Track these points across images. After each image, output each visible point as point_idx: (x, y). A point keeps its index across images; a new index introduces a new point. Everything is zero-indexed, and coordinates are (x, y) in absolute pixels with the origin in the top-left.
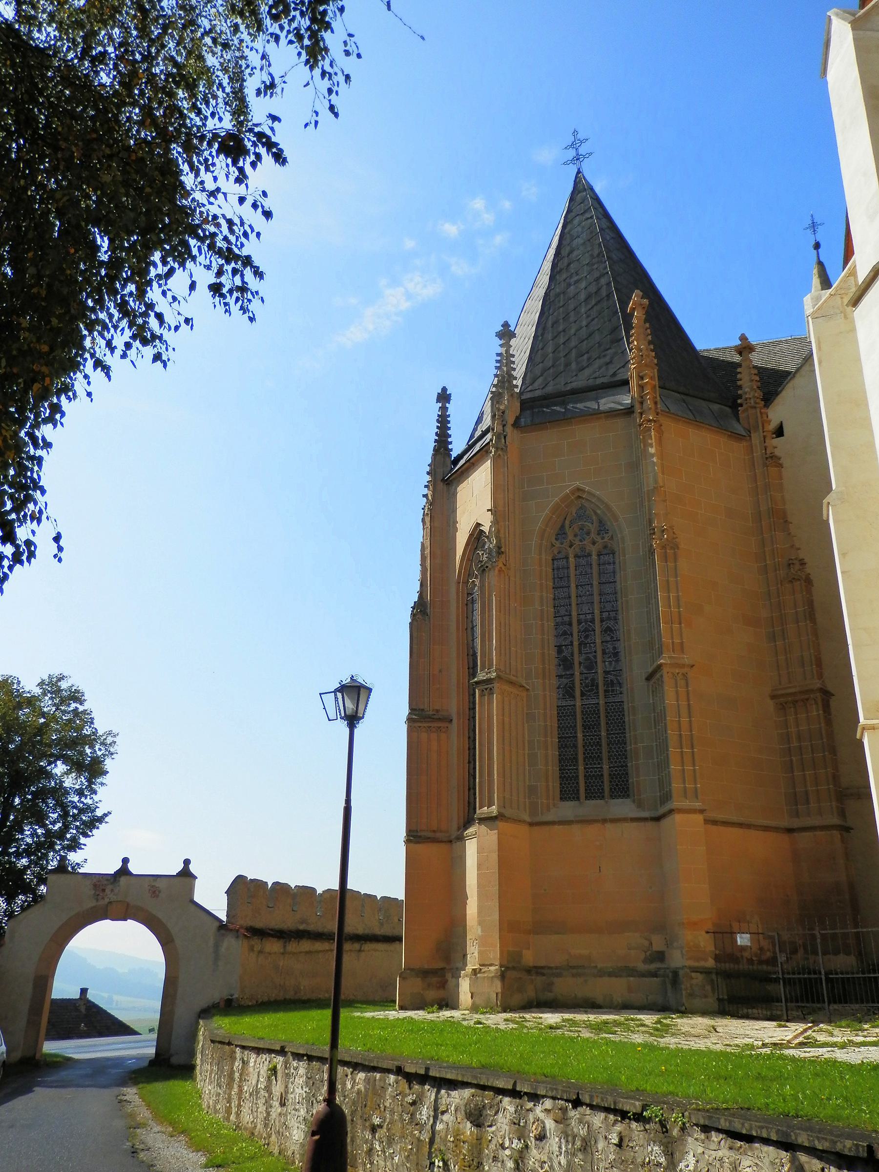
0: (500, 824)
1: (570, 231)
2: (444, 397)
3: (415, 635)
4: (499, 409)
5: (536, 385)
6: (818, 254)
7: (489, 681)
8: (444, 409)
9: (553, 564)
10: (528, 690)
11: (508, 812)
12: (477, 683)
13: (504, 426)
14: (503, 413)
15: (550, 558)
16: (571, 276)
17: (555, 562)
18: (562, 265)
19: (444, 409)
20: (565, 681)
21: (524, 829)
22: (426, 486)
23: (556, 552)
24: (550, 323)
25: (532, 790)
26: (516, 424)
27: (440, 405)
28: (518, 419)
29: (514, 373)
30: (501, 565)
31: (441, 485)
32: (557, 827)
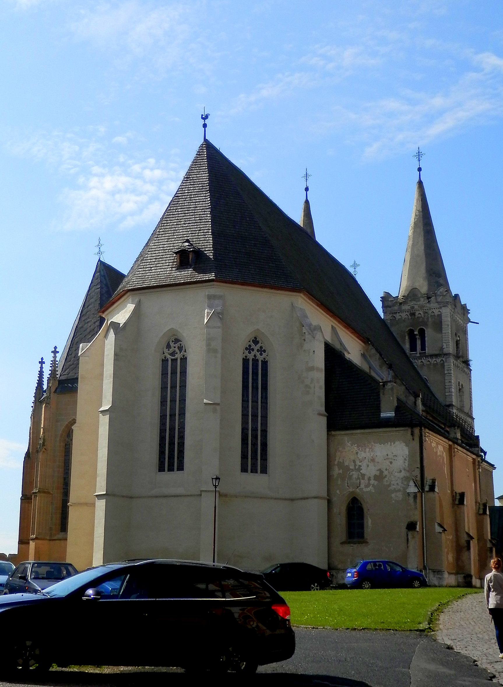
0: (37, 541)
1: (90, 294)
2: (42, 362)
3: (25, 466)
4: (49, 386)
5: (66, 372)
6: (307, 193)
7: (36, 493)
8: (41, 368)
9: (65, 447)
10: (52, 494)
11: (39, 537)
12: (33, 493)
13: (50, 393)
14: (51, 387)
15: (64, 445)
16: (86, 319)
17: (66, 446)
18: (84, 313)
19: (41, 368)
20: (65, 490)
21: (47, 542)
22: (33, 403)
23: (66, 443)
24: (75, 343)
25: (51, 529)
26: (55, 392)
27: (43, 361)
28: (57, 389)
29: (57, 369)
30: (44, 450)
31: (38, 403)
32: (57, 541)
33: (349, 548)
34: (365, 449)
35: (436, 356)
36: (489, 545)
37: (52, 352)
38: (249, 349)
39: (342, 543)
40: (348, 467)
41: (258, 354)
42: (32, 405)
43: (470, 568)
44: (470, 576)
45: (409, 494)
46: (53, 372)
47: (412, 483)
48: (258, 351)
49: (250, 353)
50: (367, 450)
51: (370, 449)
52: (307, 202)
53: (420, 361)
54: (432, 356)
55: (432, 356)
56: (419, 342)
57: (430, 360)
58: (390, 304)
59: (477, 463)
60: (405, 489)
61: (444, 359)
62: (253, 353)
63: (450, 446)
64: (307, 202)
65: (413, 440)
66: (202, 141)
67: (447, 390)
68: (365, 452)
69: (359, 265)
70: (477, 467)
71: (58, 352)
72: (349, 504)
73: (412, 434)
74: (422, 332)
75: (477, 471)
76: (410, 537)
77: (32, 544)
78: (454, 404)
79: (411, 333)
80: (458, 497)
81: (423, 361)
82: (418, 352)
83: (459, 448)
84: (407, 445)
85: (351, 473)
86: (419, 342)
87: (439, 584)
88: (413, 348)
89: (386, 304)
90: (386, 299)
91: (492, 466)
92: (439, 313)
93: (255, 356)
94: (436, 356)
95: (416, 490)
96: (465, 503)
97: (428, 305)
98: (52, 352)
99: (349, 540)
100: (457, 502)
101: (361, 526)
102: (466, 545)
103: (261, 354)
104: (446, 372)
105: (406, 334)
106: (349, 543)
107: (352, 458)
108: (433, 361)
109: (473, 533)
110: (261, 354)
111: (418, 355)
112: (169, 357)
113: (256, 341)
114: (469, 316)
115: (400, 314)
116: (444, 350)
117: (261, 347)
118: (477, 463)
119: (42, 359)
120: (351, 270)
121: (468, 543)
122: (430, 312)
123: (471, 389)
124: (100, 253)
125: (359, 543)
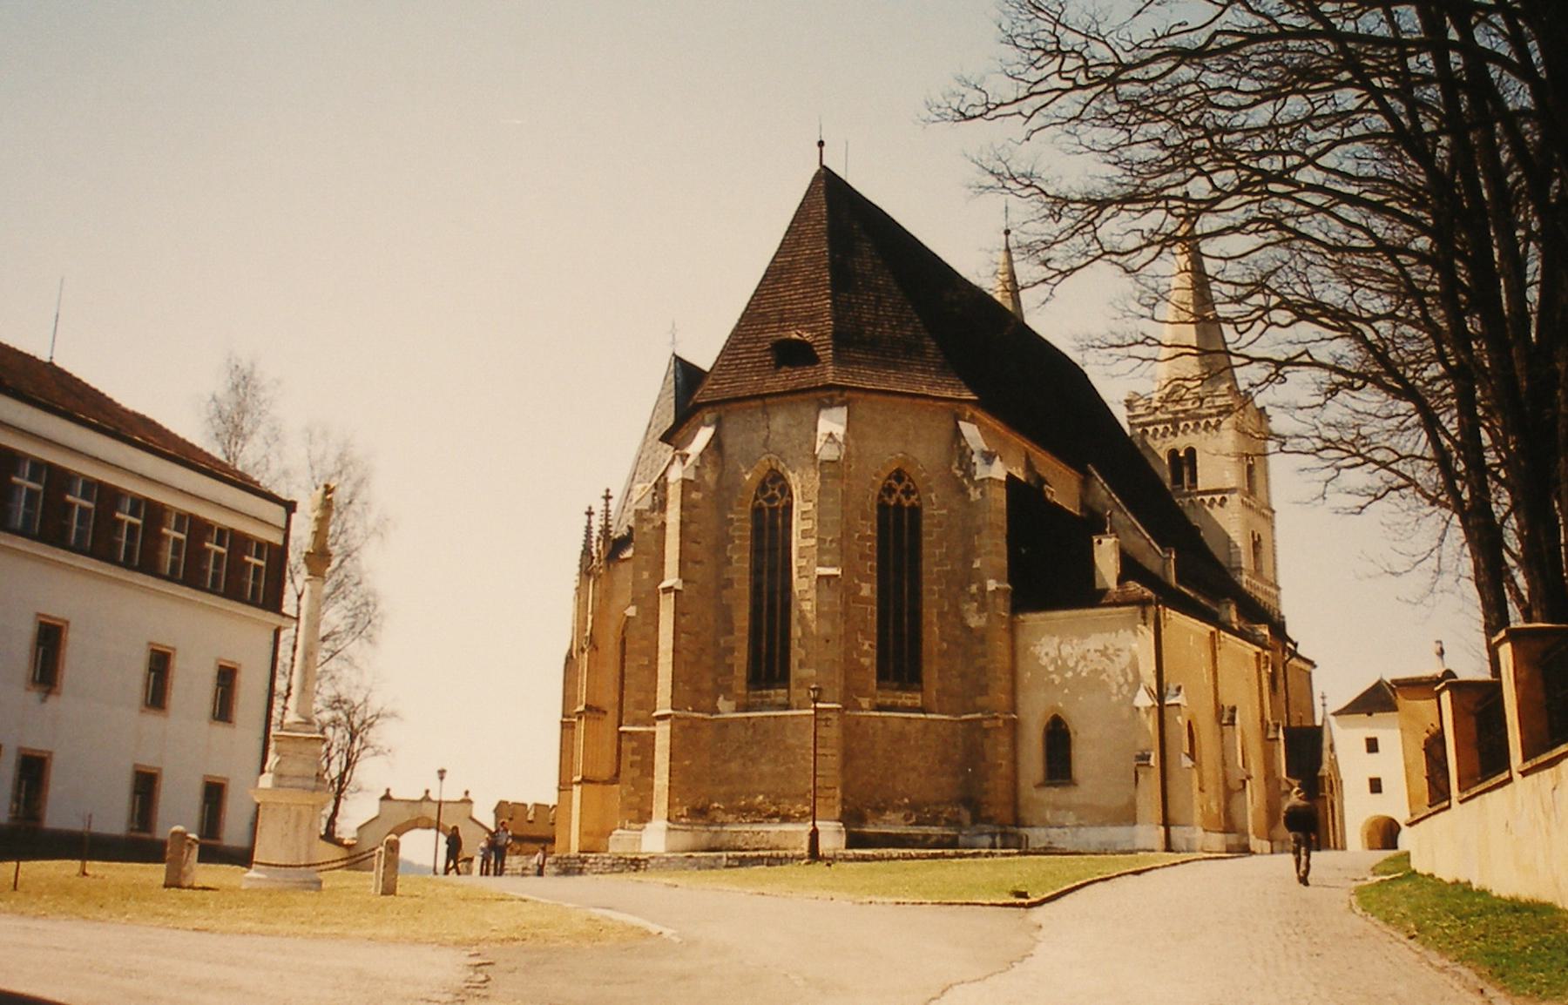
2: (590, 513)
8: (589, 522)
19: (589, 522)
38: (889, 490)
41: (903, 497)
43: (1246, 822)
44: (1246, 834)
46: (606, 530)
48: (902, 492)
49: (890, 496)
53: (1188, 499)
55: (1206, 492)
56: (1186, 470)
59: (1262, 660)
62: (894, 497)
63: (1212, 633)
66: (817, 167)
71: (611, 497)
73: (1144, 617)
74: (1191, 452)
75: (1263, 672)
76: (1141, 777)
77: (577, 790)
80: (1227, 714)
82: (1186, 485)
83: (1228, 636)
86: (1186, 470)
91: (1311, 663)
93: (899, 500)
95: (1150, 703)
96: (1237, 721)
98: (603, 497)
103: (908, 498)
106: (1048, 785)
107: (1053, 653)
109: (1256, 768)
110: (908, 498)
111: (1186, 490)
112: (765, 504)
113: (899, 475)
114: (1270, 425)
117: (908, 486)
118: (1262, 660)
119: (590, 508)
121: (1244, 782)
124: (673, 343)
125: (1063, 785)
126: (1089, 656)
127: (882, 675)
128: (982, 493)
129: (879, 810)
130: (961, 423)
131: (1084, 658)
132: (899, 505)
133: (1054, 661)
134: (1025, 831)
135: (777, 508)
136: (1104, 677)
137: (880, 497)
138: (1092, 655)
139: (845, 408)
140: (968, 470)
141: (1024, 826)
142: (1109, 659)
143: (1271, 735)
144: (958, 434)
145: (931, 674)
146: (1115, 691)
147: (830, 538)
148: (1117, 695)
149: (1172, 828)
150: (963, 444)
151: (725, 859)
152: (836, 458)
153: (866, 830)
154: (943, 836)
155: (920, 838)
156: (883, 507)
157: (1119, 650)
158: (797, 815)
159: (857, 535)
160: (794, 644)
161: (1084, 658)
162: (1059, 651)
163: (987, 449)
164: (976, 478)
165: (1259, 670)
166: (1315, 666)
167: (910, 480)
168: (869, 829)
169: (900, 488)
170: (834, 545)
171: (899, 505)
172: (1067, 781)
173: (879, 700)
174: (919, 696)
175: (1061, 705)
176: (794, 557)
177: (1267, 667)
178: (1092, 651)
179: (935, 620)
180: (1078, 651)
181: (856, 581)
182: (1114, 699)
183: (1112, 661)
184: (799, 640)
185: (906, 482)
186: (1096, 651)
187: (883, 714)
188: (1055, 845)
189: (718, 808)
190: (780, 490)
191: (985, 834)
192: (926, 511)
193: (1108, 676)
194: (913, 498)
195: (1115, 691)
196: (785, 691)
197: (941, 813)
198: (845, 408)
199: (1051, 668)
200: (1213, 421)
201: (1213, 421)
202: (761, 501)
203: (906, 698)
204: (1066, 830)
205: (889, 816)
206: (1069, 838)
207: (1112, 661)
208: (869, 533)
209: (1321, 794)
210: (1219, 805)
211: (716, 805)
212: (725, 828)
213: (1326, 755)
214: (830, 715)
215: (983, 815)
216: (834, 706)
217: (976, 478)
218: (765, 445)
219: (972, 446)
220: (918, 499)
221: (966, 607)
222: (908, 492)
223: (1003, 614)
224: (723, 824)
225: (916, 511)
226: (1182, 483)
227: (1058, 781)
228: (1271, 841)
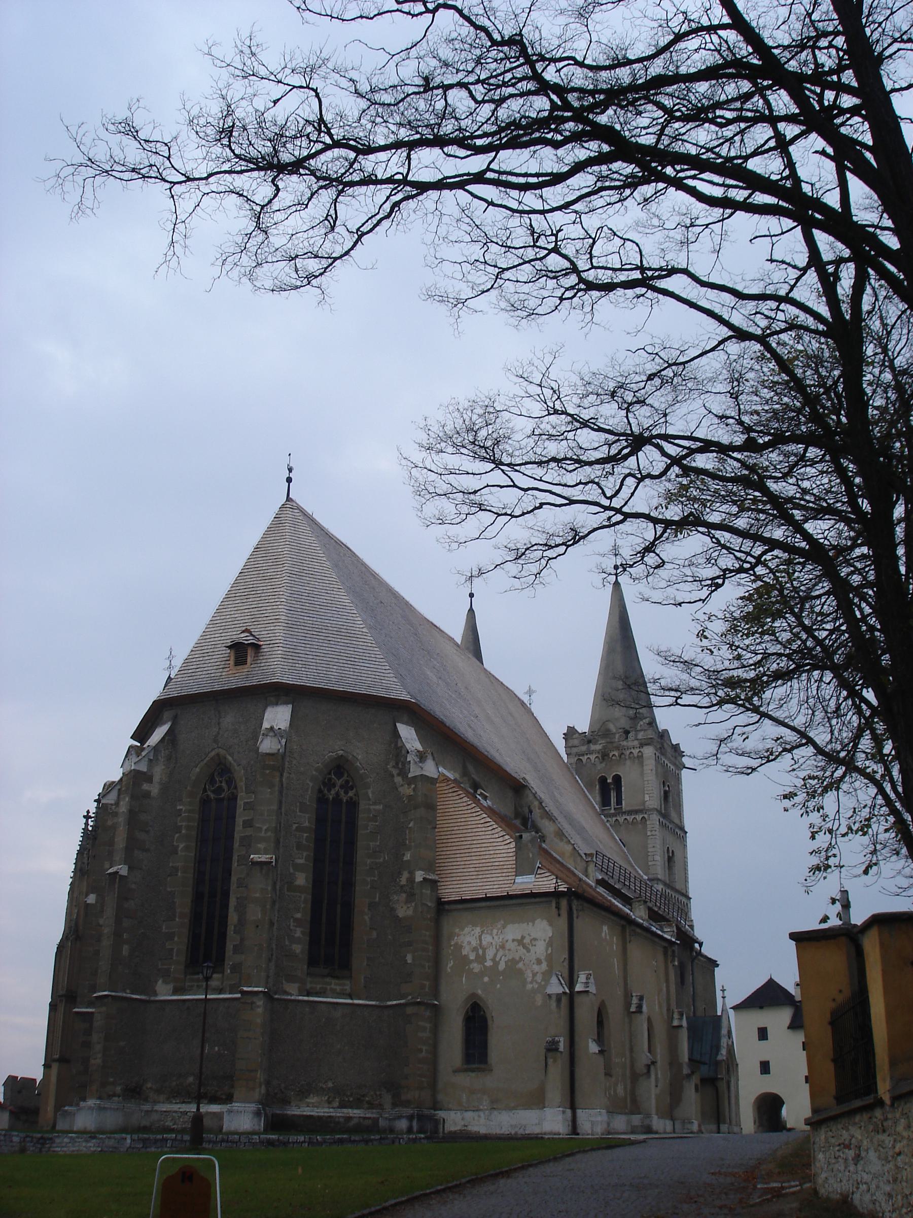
33: (465, 1080)
34: (492, 930)
35: (636, 812)
36: (686, 1070)
37: (95, 801)
38: (330, 785)
39: (455, 1072)
40: (466, 957)
41: (342, 792)
42: (72, 875)
45: (550, 996)
47: (554, 980)
48: (334, 785)
49: (329, 790)
50: (495, 931)
51: (498, 929)
52: (471, 610)
53: (614, 819)
54: (630, 812)
55: (630, 812)
56: (613, 795)
57: (628, 818)
58: (576, 742)
60: (545, 987)
61: (646, 816)
62: (333, 792)
64: (471, 610)
65: (559, 915)
67: (650, 858)
68: (491, 934)
69: (535, 692)
70: (670, 959)
72: (467, 1012)
73: (558, 908)
74: (617, 779)
76: (550, 1061)
78: (659, 877)
79: (603, 780)
80: (635, 1001)
81: (618, 818)
84: (551, 925)
85: (471, 966)
86: (613, 795)
87: (592, 1130)
88: (605, 802)
89: (571, 743)
90: (570, 734)
92: (640, 754)
93: (337, 794)
94: (636, 812)
95: (560, 990)
96: (645, 1008)
97: (625, 743)
98: (95, 801)
99: (466, 1066)
100: (633, 1009)
101: (484, 1045)
102: (645, 1071)
103: (346, 793)
104: (649, 833)
105: (597, 783)
106: (466, 1070)
107: (474, 943)
108: (630, 818)
110: (346, 793)
111: (612, 811)
112: (212, 796)
115: (588, 756)
116: (647, 803)
117: (347, 782)
120: (525, 699)
121: (648, 1067)
122: (628, 752)
123: (686, 857)
125: (483, 1070)
126: (508, 946)
127: (313, 962)
128: (414, 790)
129: (303, 1094)
130: (398, 724)
131: (503, 947)
132: (337, 800)
133: (475, 949)
134: (441, 1114)
135: (223, 799)
136: (520, 965)
137: (320, 791)
138: (511, 945)
139: (290, 706)
140: (404, 772)
141: (441, 1110)
142: (524, 947)
143: (676, 1023)
144: (396, 735)
145: (359, 961)
146: (529, 979)
147: (265, 828)
148: (531, 983)
149: (579, 1112)
150: (400, 744)
151: (129, 1141)
152: (276, 751)
153: (289, 1112)
154: (365, 1118)
155: (342, 1120)
156: (321, 800)
157: (535, 939)
158: (224, 1097)
159: (295, 826)
160: (231, 929)
161: (503, 947)
162: (480, 940)
163: (420, 748)
164: (410, 776)
165: (666, 962)
166: (718, 965)
167: (349, 775)
168: (295, 1110)
169: (339, 782)
170: (269, 834)
171: (337, 800)
172: (482, 1066)
173: (309, 986)
174: (348, 982)
175: (480, 992)
176: (236, 845)
177: (673, 961)
178: (510, 941)
179: (366, 910)
180: (498, 940)
181: (292, 871)
182: (529, 987)
183: (528, 951)
184: (235, 926)
185: (345, 777)
186: (513, 940)
187: (311, 999)
188: (470, 1128)
189: (151, 1088)
190: (227, 782)
191: (404, 1117)
192: (363, 805)
193: (524, 965)
194: (351, 794)
195: (529, 979)
196: (220, 976)
197: (364, 1096)
198: (290, 706)
199: (472, 957)
200: (636, 752)
201: (636, 752)
202: (209, 793)
203: (334, 984)
204: (482, 1114)
205: (313, 1099)
206: (482, 1121)
207: (528, 951)
208: (307, 824)
209: (719, 1076)
210: (625, 1088)
211: (149, 1085)
212: (157, 1107)
213: (724, 1041)
214: (255, 999)
215: (403, 1098)
216: (260, 989)
217: (410, 776)
218: (215, 741)
219: (408, 746)
220: (356, 795)
221: (396, 897)
222: (347, 787)
223: (429, 904)
224: (155, 1102)
225: (353, 805)
226: (610, 805)
227: (475, 1066)
228: (673, 1119)
